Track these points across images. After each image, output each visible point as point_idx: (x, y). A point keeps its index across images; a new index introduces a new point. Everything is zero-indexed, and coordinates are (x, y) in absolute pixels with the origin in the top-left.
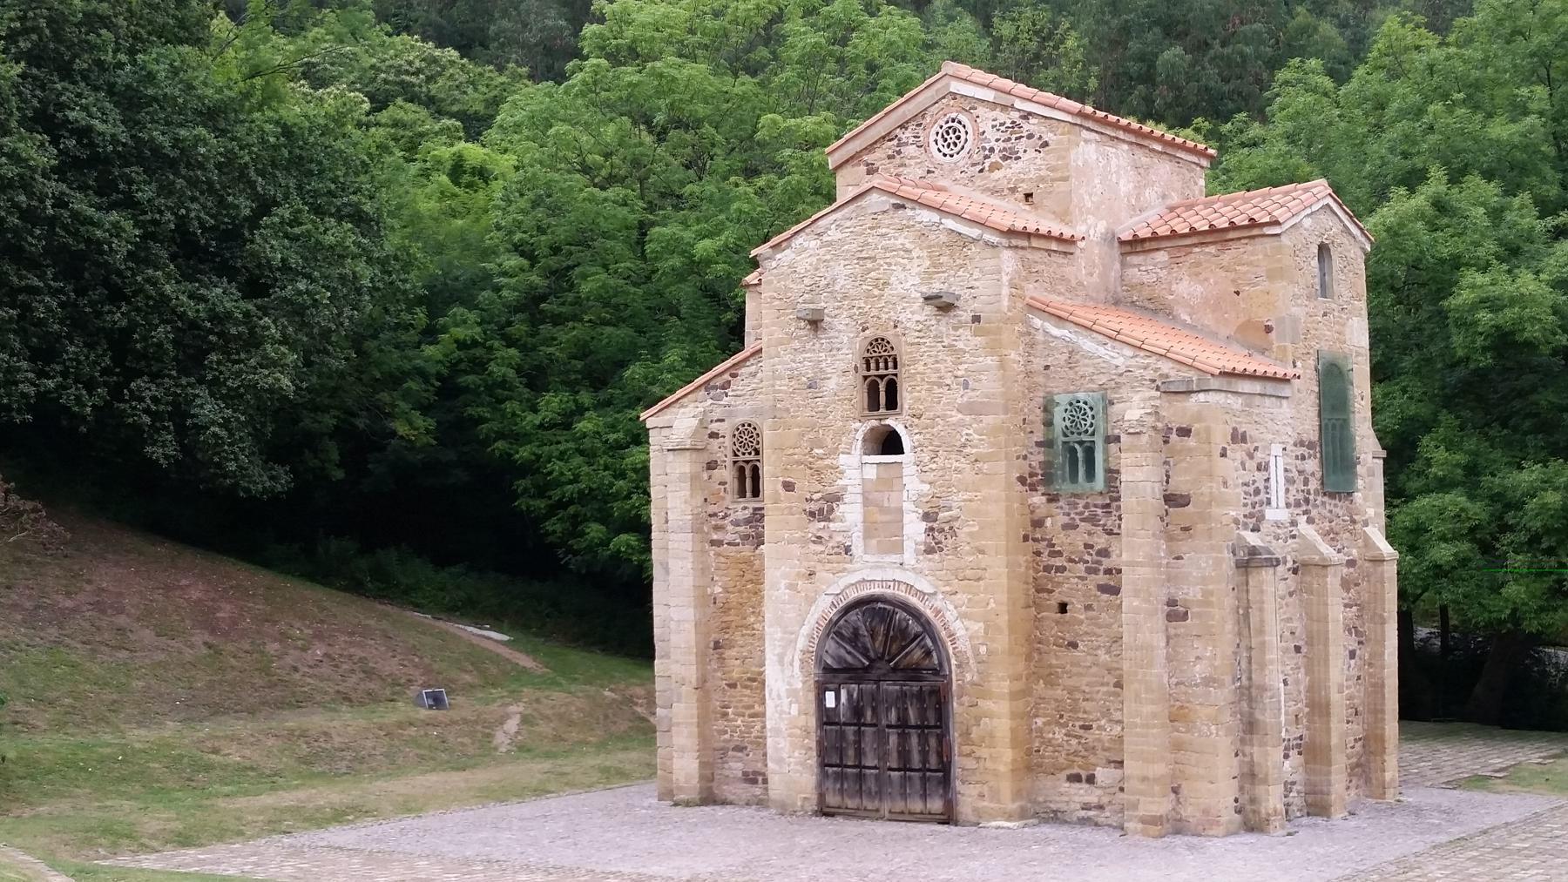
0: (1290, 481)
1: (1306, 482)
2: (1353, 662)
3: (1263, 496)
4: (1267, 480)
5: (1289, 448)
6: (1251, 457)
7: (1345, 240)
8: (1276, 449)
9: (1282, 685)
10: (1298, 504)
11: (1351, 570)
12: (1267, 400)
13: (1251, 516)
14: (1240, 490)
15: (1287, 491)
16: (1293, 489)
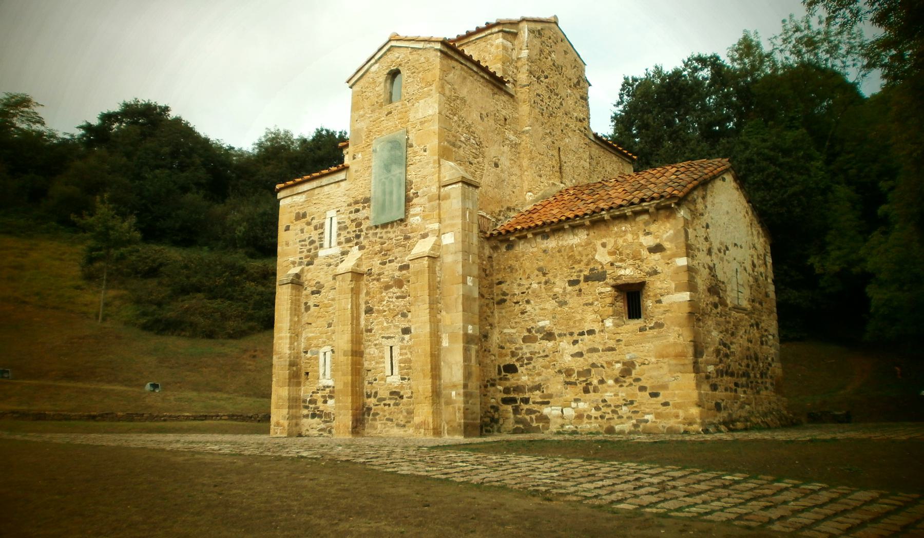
0: (342, 228)
1: (359, 225)
2: (407, 337)
3: (317, 244)
4: (322, 233)
5: (342, 210)
6: (309, 224)
7: (415, 56)
8: (332, 213)
9: (329, 354)
10: (348, 241)
11: (404, 272)
12: (326, 188)
13: (307, 257)
14: (298, 245)
15: (339, 235)
16: (344, 233)
